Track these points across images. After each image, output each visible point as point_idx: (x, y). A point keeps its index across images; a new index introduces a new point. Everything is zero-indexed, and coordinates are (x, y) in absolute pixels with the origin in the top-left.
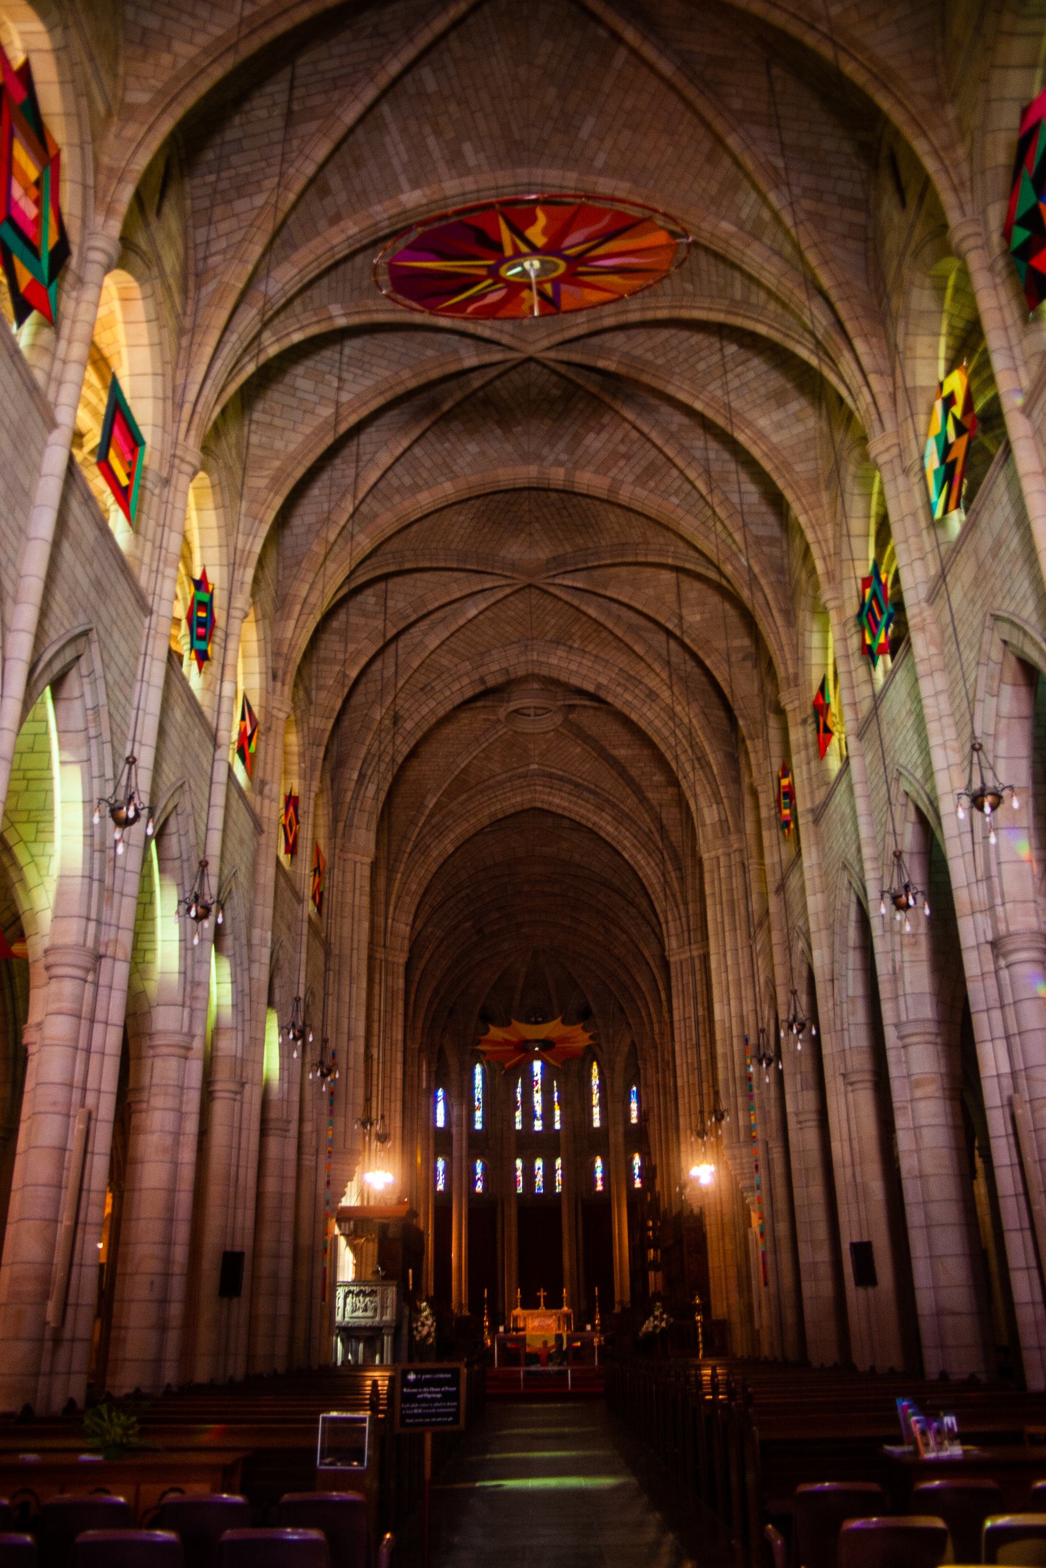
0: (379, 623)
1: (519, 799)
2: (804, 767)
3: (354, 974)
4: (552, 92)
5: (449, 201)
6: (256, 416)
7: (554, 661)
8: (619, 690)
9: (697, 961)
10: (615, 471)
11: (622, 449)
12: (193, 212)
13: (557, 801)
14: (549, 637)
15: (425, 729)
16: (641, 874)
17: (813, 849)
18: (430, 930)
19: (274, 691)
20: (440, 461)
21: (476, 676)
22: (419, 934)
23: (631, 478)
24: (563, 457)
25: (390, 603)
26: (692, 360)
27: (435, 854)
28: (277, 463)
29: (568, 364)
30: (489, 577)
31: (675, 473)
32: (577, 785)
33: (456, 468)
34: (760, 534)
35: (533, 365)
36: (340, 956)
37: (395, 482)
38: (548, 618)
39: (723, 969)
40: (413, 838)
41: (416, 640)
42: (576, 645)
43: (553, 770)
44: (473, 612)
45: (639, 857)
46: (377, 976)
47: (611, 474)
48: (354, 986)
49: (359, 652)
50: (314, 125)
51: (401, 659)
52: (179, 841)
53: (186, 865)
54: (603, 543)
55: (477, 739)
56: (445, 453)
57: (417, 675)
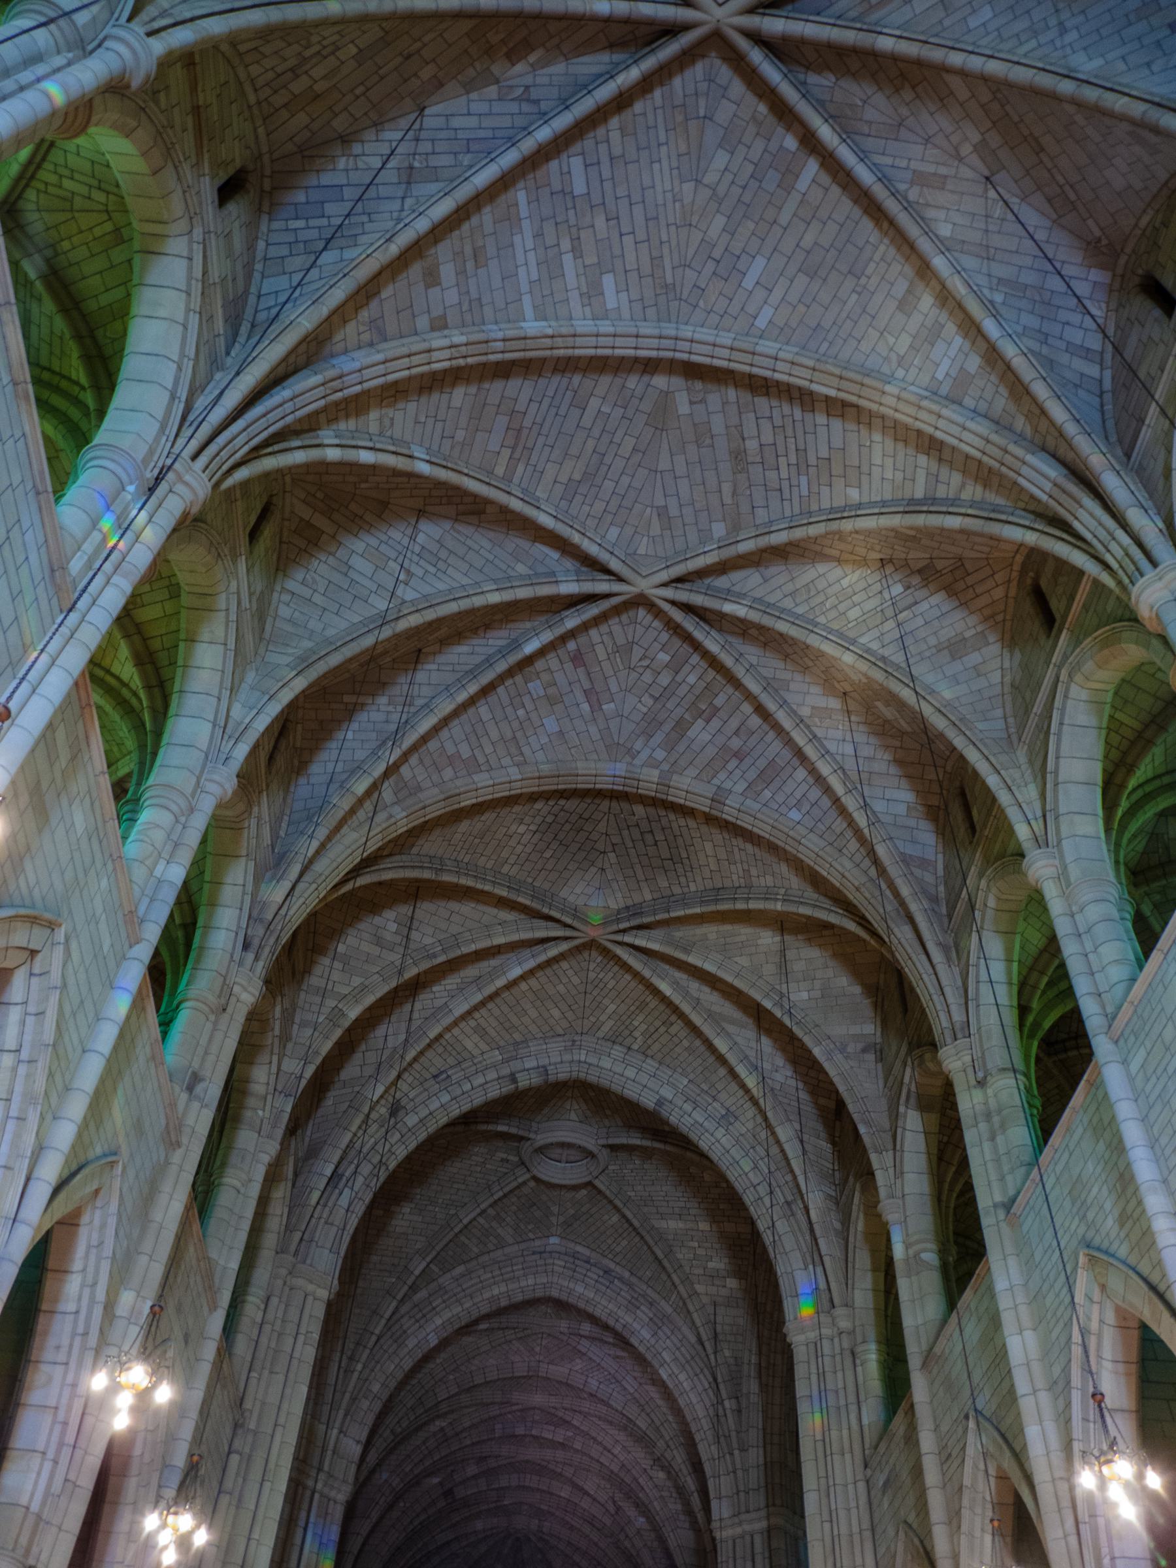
0: (395, 957)
1: (531, 1282)
2: (987, 1145)
3: (271, 1465)
4: (720, 221)
5: (579, 341)
6: (291, 585)
7: (606, 1063)
8: (688, 1107)
9: (758, 1540)
10: (722, 776)
11: (736, 743)
12: (265, 259)
13: (580, 1289)
14: (600, 1034)
15: (431, 1130)
16: (681, 1402)
17: (1012, 1262)
18: (385, 1476)
19: (241, 963)
20: (509, 735)
21: (506, 1071)
22: (372, 1472)
23: (740, 787)
24: (660, 754)
25: (415, 935)
26: (842, 607)
27: (411, 1343)
28: (307, 644)
29: (687, 608)
30: (543, 923)
31: (801, 773)
32: (607, 1272)
33: (526, 750)
34: (908, 851)
35: (642, 612)
36: (255, 1433)
37: (450, 749)
38: (606, 1001)
39: (826, 1517)
40: (387, 1315)
41: (438, 1003)
42: (635, 1047)
43: (579, 1248)
44: (516, 972)
45: (682, 1377)
46: (303, 1514)
47: (715, 781)
48: (267, 1485)
49: (364, 988)
50: (433, 187)
51: (415, 1024)
52: (23, 1023)
53: (22, 1070)
54: (693, 888)
55: (489, 1187)
56: (515, 724)
57: (430, 1054)
